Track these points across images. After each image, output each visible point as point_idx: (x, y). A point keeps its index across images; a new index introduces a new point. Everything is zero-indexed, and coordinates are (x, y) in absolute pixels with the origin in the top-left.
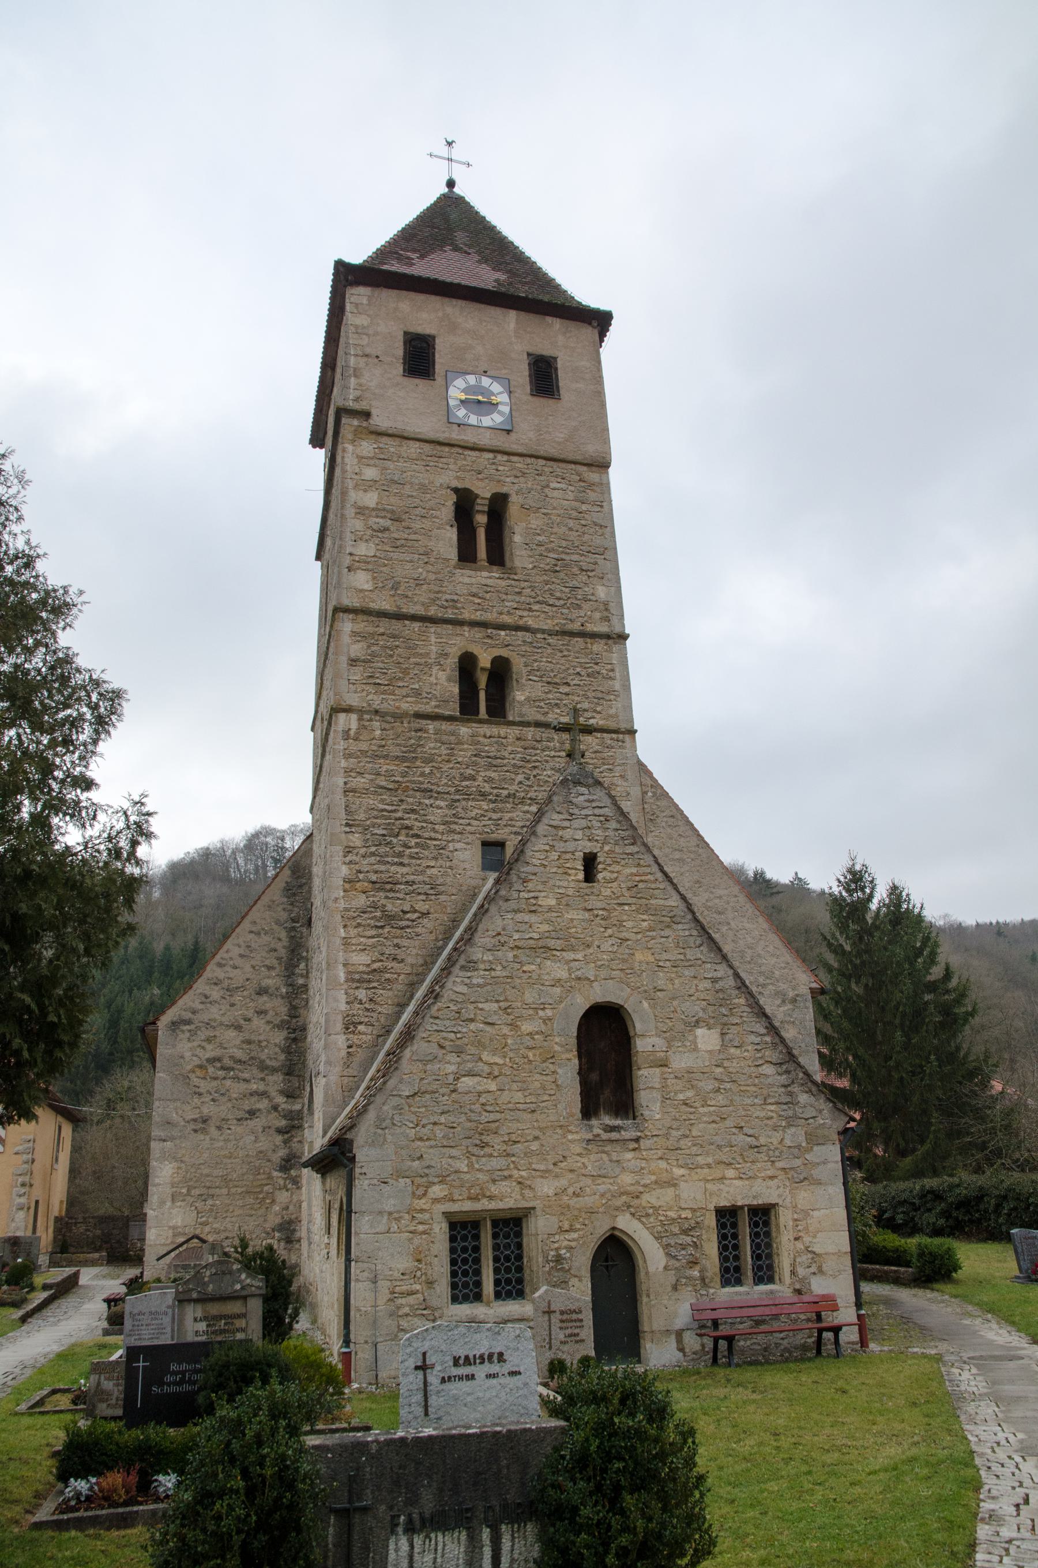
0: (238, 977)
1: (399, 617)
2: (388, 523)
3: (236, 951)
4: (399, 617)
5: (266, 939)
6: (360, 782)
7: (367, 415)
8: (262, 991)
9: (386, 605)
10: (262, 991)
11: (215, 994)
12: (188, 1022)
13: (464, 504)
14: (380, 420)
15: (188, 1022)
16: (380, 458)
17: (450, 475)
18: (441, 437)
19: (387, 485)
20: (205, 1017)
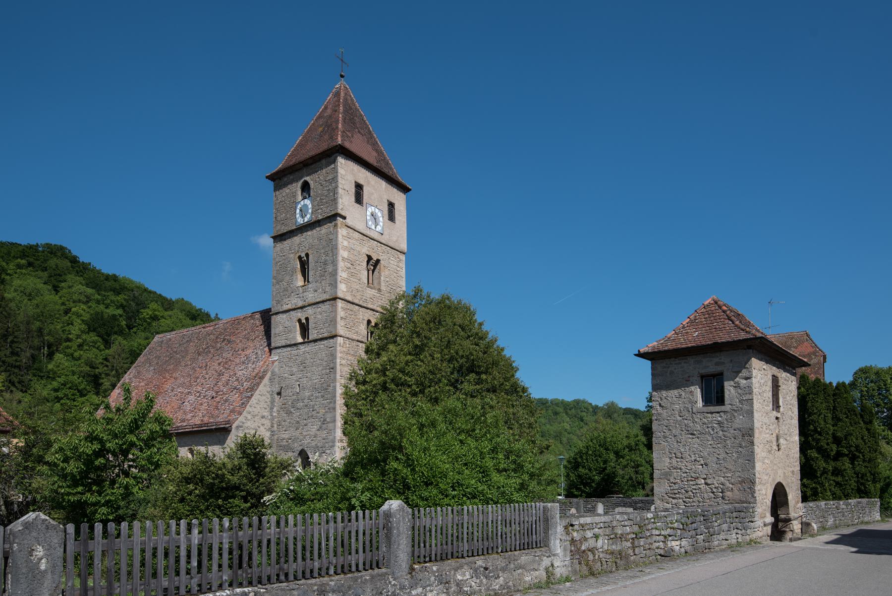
0: (256, 411)
1: (353, 303)
2: (349, 265)
3: (255, 401)
4: (353, 303)
5: (264, 398)
6: (344, 362)
7: (344, 218)
8: (263, 417)
9: (349, 298)
10: (263, 417)
11: (249, 417)
12: (241, 427)
13: (369, 258)
14: (349, 221)
15: (241, 427)
16: (349, 238)
17: (366, 248)
18: (364, 232)
19: (350, 249)
20: (246, 425)
